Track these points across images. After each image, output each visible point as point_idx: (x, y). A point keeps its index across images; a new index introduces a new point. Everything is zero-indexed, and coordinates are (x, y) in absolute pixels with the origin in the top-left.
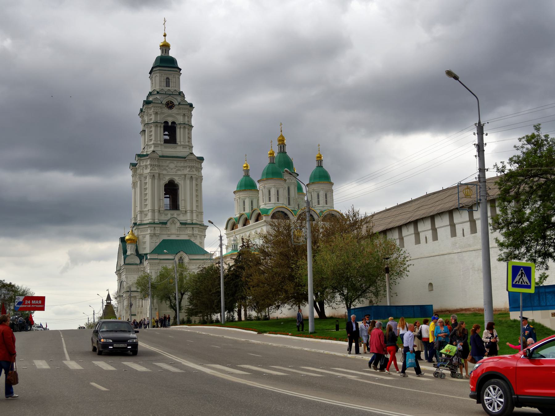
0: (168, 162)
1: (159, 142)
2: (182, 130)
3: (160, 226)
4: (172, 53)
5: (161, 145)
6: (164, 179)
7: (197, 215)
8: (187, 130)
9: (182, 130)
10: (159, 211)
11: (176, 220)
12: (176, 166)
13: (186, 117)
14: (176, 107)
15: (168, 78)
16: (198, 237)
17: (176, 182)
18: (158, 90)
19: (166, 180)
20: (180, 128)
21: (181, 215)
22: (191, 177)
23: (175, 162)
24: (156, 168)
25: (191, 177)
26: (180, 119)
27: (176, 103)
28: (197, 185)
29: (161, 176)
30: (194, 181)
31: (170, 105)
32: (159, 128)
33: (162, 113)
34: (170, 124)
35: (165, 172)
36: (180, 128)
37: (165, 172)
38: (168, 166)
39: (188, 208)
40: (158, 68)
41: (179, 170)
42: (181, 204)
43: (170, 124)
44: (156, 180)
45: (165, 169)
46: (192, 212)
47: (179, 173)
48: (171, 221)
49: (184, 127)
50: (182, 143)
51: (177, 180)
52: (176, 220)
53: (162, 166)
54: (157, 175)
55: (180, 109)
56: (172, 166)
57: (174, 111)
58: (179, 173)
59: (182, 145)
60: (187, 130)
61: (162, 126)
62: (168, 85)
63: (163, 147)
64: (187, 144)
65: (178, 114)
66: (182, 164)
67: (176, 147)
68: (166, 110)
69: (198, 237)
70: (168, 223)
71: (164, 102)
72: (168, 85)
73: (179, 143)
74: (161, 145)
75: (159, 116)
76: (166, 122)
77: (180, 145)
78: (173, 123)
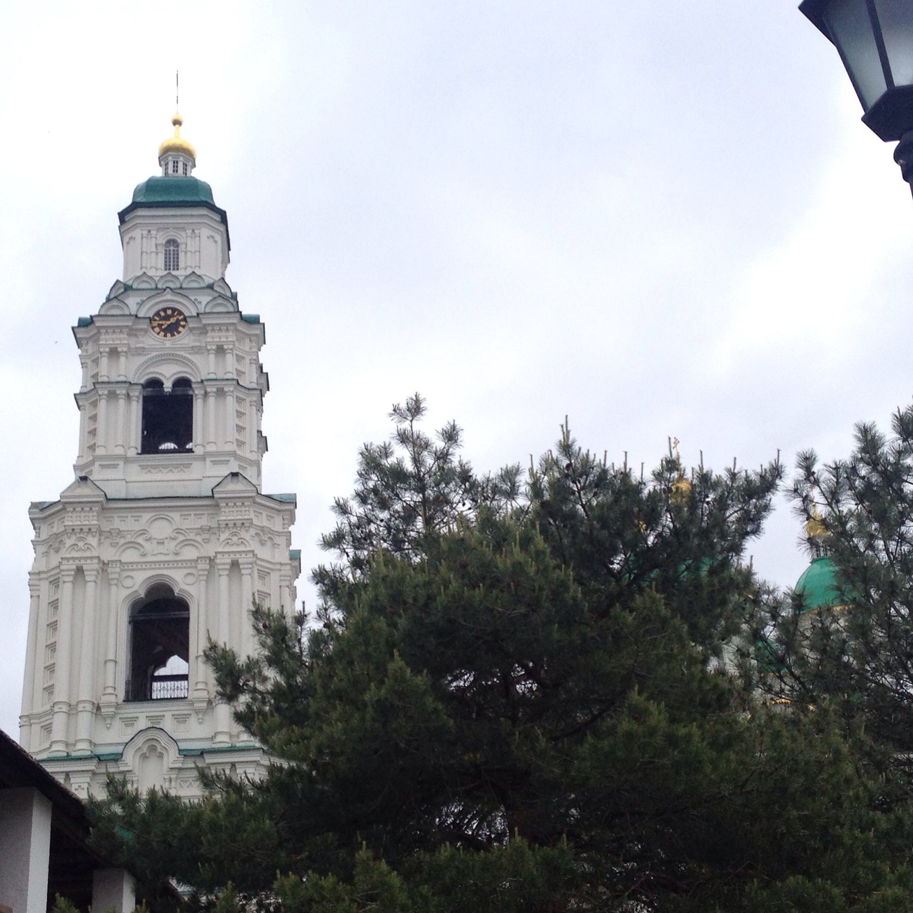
0: (146, 516)
1: (119, 451)
2: (212, 400)
3: (91, 766)
4: (198, 173)
5: (127, 460)
6: (128, 582)
10: (98, 708)
11: (163, 740)
12: (178, 531)
13: (230, 358)
14: (192, 324)
17: (176, 591)
18: (130, 283)
19: (137, 584)
20: (206, 394)
21: (193, 720)
22: (235, 565)
23: (176, 516)
24: (93, 541)
25: (235, 565)
26: (204, 367)
27: (189, 310)
29: (113, 570)
30: (246, 580)
31: (170, 322)
32: (122, 402)
33: (139, 352)
34: (168, 387)
35: (130, 556)
36: (206, 394)
37: (130, 556)
38: (143, 532)
40: (141, 212)
41: (187, 543)
43: (168, 387)
44: (91, 587)
47: (189, 553)
48: (140, 741)
49: (221, 393)
50: (211, 448)
51: (183, 583)
52: (163, 740)
53: (120, 533)
54: (91, 567)
55: (204, 330)
56: (161, 529)
57: (185, 339)
58: (189, 553)
59: (211, 454)
60: (230, 401)
61: (137, 393)
63: (134, 468)
65: (197, 350)
66: (204, 521)
67: (188, 466)
73: (198, 451)
74: (127, 460)
75: (123, 359)
76: (155, 384)
77: (203, 458)
78: (183, 383)
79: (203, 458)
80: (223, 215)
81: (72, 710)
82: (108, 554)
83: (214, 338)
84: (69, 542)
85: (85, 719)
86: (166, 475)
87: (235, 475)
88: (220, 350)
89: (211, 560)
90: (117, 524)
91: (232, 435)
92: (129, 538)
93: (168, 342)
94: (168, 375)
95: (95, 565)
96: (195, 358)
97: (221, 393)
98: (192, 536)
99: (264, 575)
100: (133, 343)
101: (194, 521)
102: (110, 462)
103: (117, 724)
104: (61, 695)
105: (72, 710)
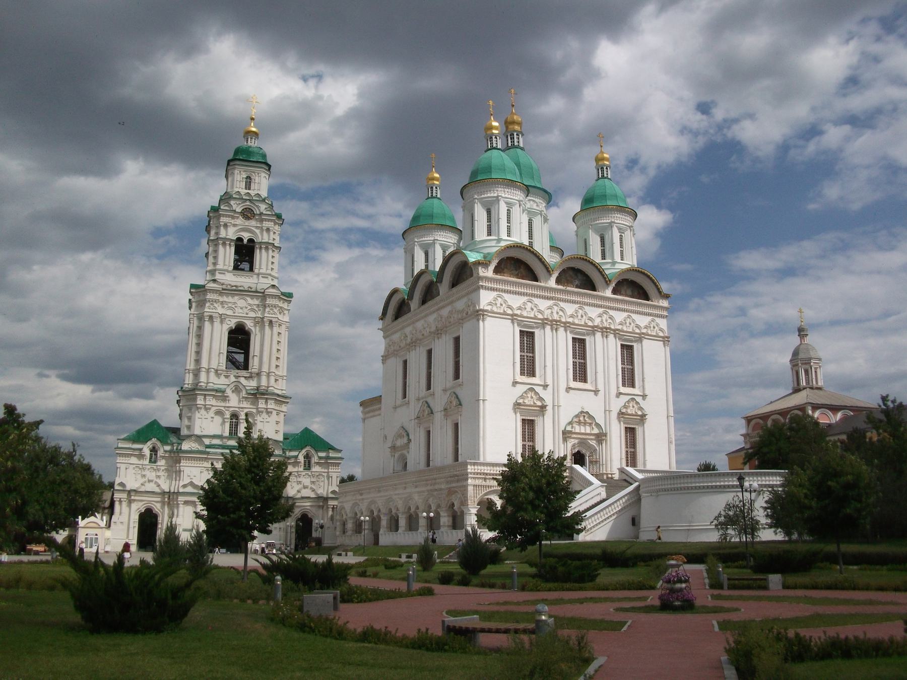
0: (236, 298)
1: (226, 268)
2: (263, 251)
7: (276, 380)
8: (270, 251)
9: (263, 251)
12: (250, 305)
13: (272, 233)
15: (249, 178)
16: (274, 412)
19: (232, 323)
20: (261, 248)
22: (271, 322)
23: (248, 299)
25: (271, 322)
28: (279, 333)
32: (228, 247)
33: (235, 225)
34: (245, 241)
35: (230, 312)
38: (235, 303)
39: (265, 369)
41: (253, 310)
42: (254, 363)
43: (245, 241)
44: (215, 324)
45: (230, 308)
46: (268, 375)
49: (267, 249)
50: (261, 271)
56: (241, 303)
57: (253, 223)
58: (252, 314)
60: (270, 251)
61: (233, 244)
62: (248, 186)
64: (269, 272)
68: (240, 221)
69: (274, 412)
70: (229, 392)
71: (239, 210)
72: (248, 186)
74: (228, 271)
76: (240, 239)
78: (251, 241)
79: (258, 275)
80: (269, 166)
81: (208, 371)
82: (221, 310)
83: (266, 224)
84: (208, 304)
85: (212, 374)
86: (244, 280)
87: (273, 286)
88: (268, 230)
89: (263, 318)
90: (225, 299)
91: (270, 266)
92: (230, 305)
93: (247, 223)
94: (246, 236)
95: (217, 315)
96: (258, 231)
97: (267, 249)
98: (255, 307)
99: (280, 325)
100: (233, 221)
101: (256, 302)
102: (223, 271)
103: (222, 377)
104: (204, 364)
105: (208, 371)
